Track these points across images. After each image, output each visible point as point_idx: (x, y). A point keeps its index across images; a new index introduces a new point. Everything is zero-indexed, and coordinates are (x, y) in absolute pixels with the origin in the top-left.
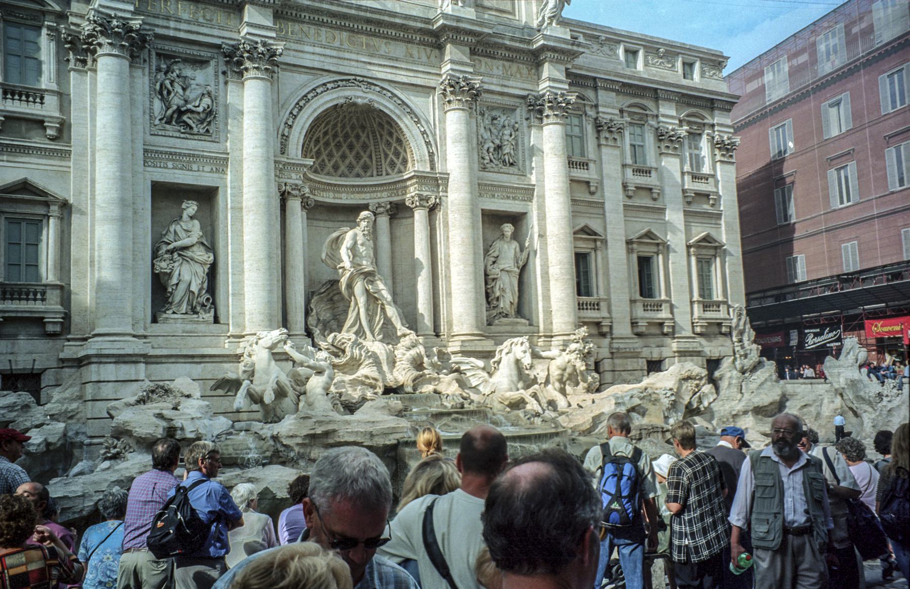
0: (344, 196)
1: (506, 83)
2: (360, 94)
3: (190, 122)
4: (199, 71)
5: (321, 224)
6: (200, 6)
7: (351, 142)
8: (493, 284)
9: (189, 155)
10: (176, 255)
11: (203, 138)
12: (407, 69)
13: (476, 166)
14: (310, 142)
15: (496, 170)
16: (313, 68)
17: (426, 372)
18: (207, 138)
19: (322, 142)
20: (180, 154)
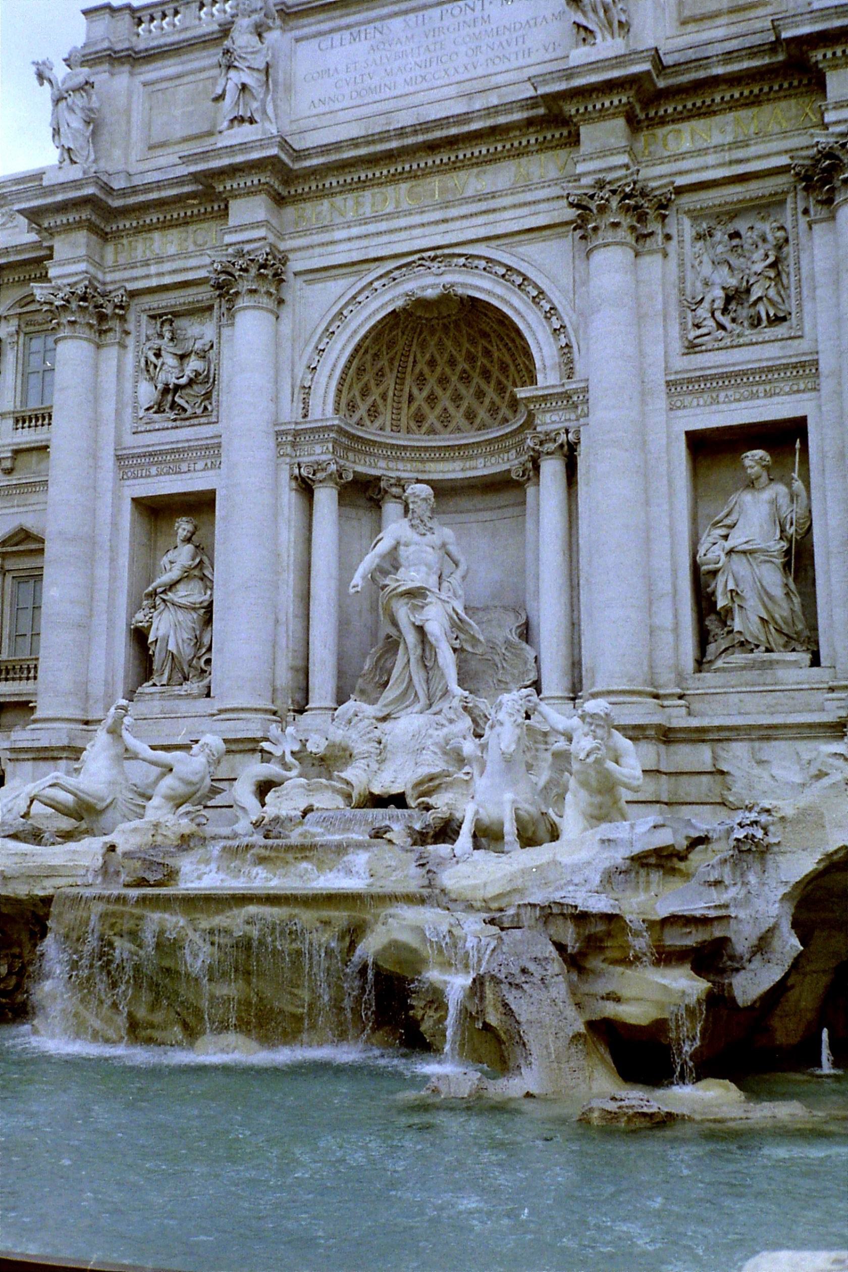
0: (480, 462)
1: (740, 154)
2: (430, 280)
3: (181, 402)
4: (208, 323)
5: (472, 517)
6: (191, 228)
7: (483, 366)
8: (713, 586)
9: (172, 451)
10: (158, 601)
11: (195, 421)
12: (514, 206)
13: (663, 348)
14: (403, 384)
15: (727, 342)
16: (353, 264)
17: (467, 769)
18: (202, 420)
19: (432, 381)
20: (161, 453)
